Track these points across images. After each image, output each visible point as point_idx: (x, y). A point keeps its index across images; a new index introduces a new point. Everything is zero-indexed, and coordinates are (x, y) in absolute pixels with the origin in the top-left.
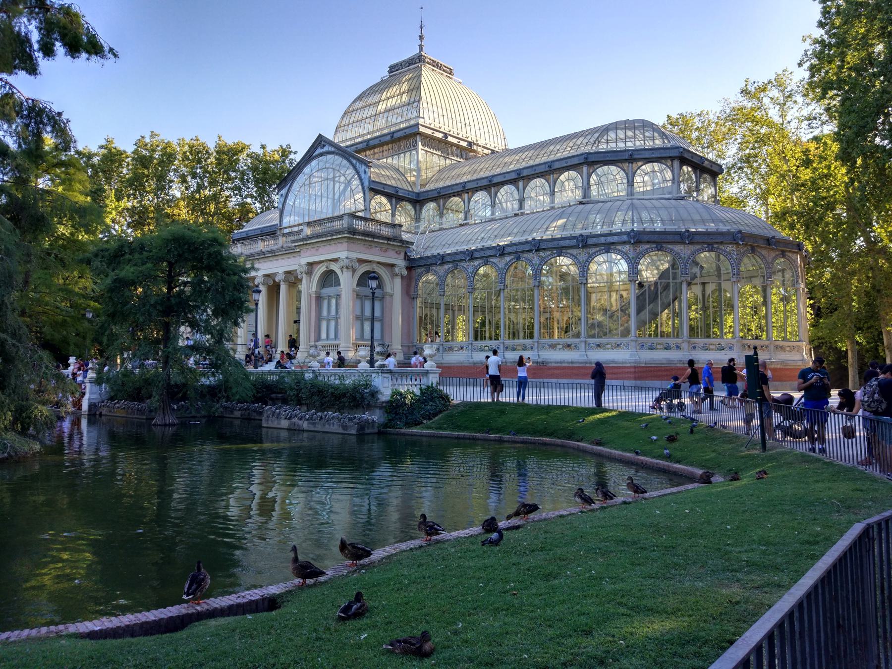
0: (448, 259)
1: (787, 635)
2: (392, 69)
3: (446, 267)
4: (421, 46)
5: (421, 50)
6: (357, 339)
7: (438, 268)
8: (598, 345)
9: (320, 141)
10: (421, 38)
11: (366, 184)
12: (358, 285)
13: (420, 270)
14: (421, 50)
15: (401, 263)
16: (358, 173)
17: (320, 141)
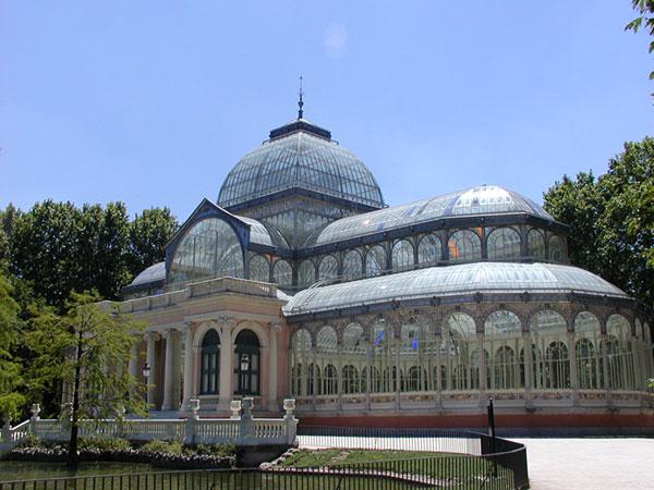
0: (319, 316)
1: (276, 485)
2: (275, 135)
3: (317, 324)
4: (301, 112)
5: (300, 117)
6: (235, 393)
7: (311, 324)
8: (452, 397)
9: (206, 203)
10: (301, 104)
11: (246, 244)
12: (236, 343)
13: (296, 326)
14: (300, 117)
15: (276, 319)
16: (238, 235)
17: (206, 203)
